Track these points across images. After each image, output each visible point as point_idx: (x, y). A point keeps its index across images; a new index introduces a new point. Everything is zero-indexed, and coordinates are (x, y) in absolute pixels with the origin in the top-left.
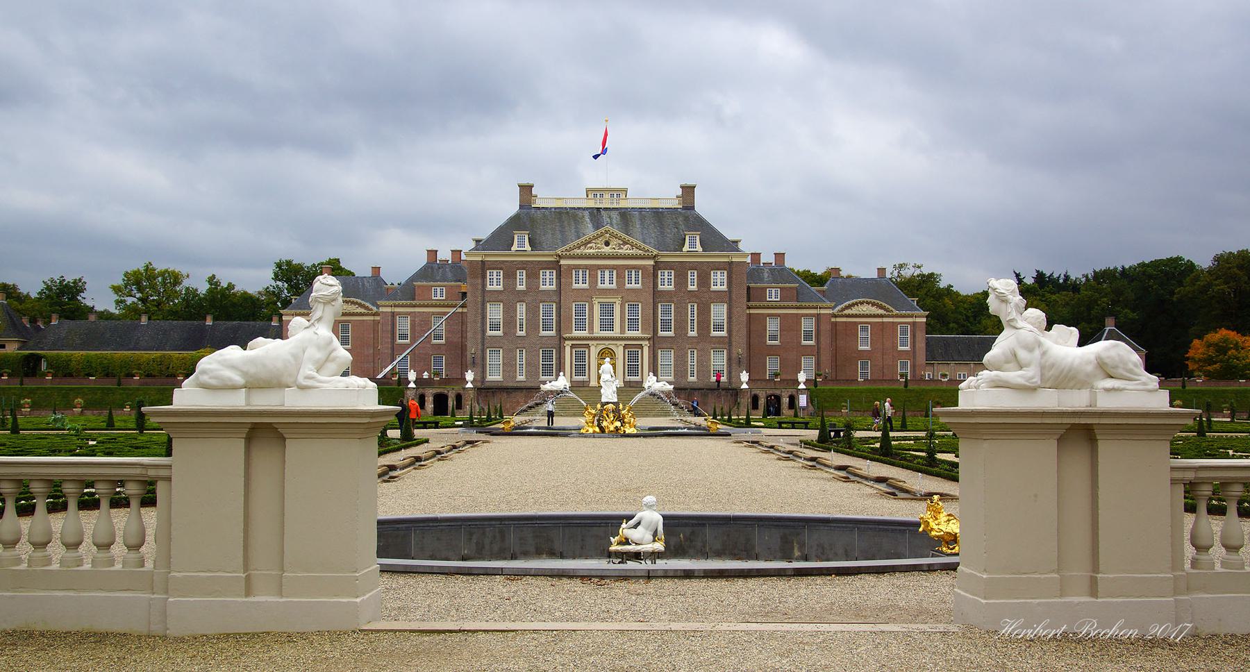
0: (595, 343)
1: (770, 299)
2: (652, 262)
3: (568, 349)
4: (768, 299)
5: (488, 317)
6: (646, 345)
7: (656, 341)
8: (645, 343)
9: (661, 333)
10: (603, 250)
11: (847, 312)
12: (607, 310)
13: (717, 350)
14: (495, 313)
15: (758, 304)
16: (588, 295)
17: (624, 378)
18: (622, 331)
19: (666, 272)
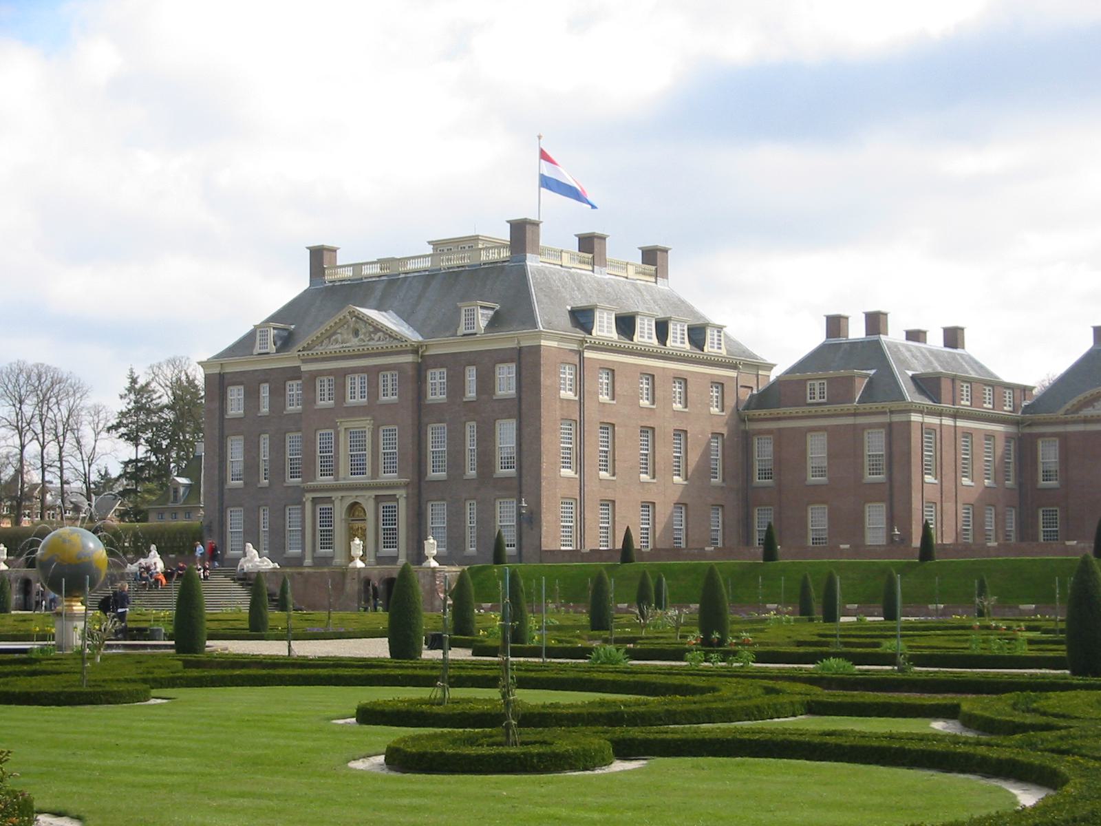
0: (340, 494)
1: (813, 401)
2: (409, 358)
3: (308, 506)
4: (809, 401)
5: (229, 459)
6: (401, 496)
7: (420, 490)
8: (401, 493)
9: (432, 475)
10: (348, 345)
11: (1088, 412)
12: (357, 439)
13: (505, 500)
14: (236, 451)
15: (793, 410)
16: (329, 418)
17: (377, 549)
18: (375, 473)
19: (437, 371)
